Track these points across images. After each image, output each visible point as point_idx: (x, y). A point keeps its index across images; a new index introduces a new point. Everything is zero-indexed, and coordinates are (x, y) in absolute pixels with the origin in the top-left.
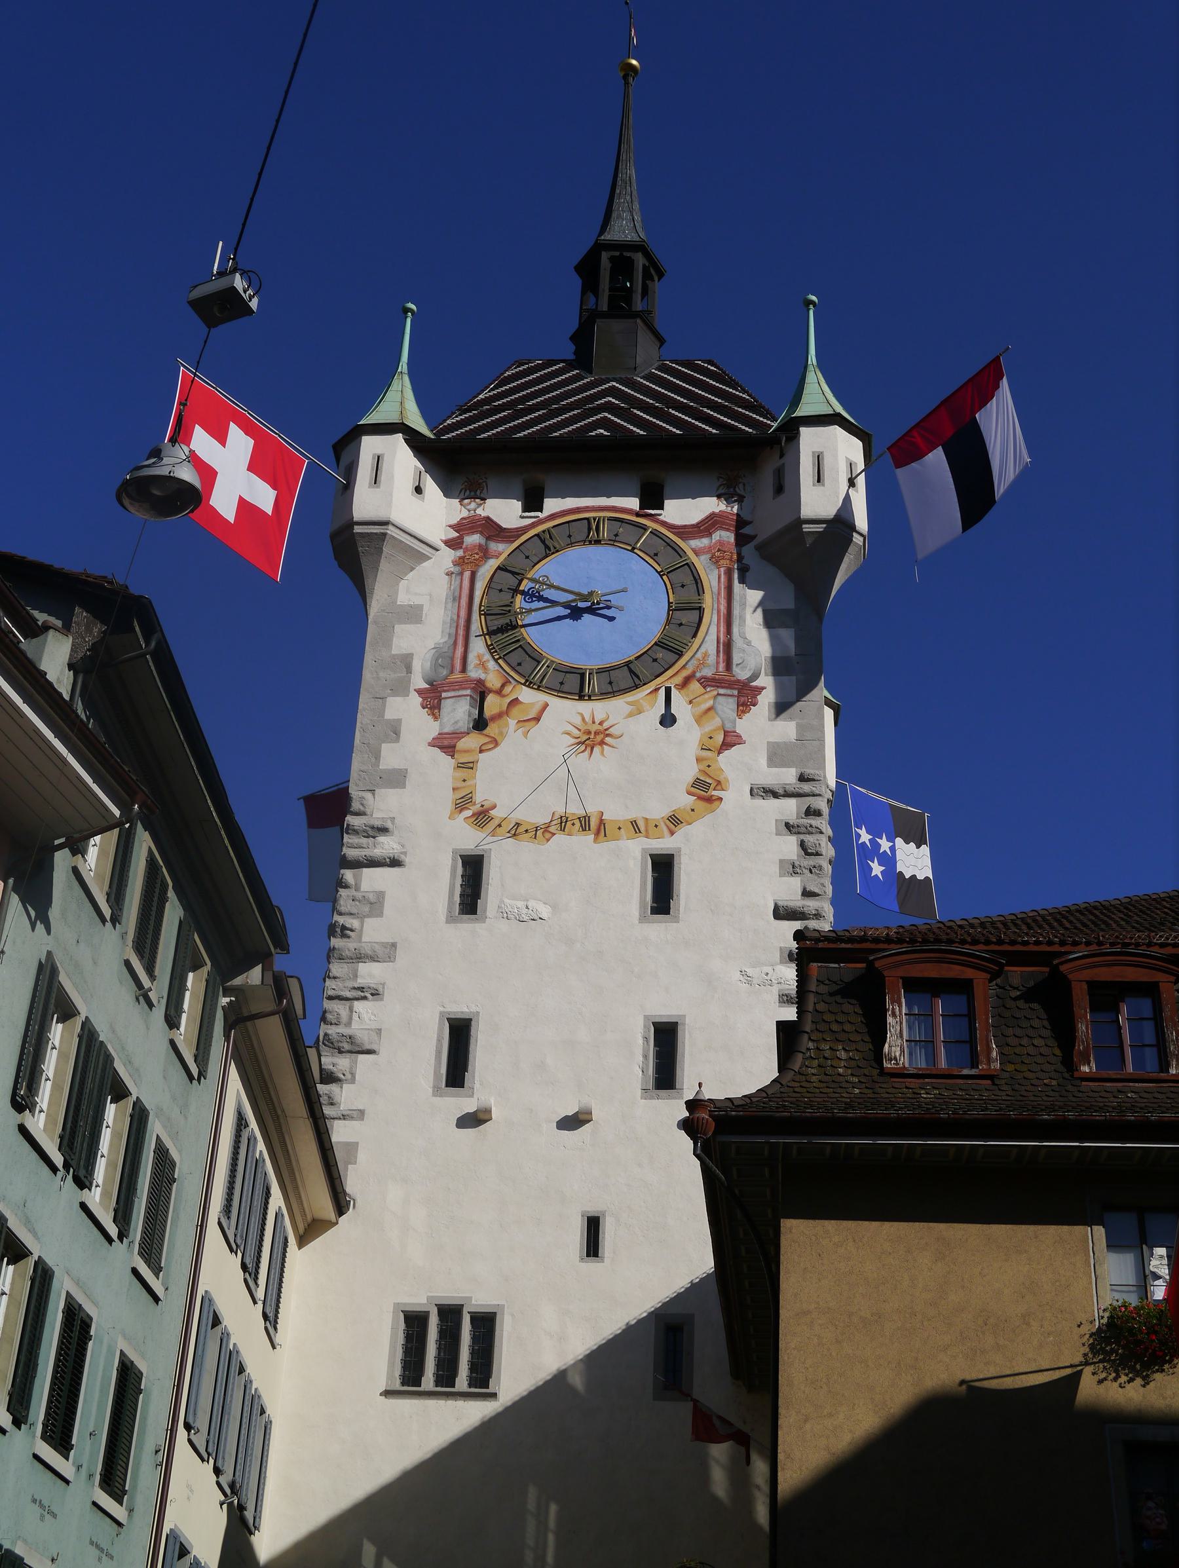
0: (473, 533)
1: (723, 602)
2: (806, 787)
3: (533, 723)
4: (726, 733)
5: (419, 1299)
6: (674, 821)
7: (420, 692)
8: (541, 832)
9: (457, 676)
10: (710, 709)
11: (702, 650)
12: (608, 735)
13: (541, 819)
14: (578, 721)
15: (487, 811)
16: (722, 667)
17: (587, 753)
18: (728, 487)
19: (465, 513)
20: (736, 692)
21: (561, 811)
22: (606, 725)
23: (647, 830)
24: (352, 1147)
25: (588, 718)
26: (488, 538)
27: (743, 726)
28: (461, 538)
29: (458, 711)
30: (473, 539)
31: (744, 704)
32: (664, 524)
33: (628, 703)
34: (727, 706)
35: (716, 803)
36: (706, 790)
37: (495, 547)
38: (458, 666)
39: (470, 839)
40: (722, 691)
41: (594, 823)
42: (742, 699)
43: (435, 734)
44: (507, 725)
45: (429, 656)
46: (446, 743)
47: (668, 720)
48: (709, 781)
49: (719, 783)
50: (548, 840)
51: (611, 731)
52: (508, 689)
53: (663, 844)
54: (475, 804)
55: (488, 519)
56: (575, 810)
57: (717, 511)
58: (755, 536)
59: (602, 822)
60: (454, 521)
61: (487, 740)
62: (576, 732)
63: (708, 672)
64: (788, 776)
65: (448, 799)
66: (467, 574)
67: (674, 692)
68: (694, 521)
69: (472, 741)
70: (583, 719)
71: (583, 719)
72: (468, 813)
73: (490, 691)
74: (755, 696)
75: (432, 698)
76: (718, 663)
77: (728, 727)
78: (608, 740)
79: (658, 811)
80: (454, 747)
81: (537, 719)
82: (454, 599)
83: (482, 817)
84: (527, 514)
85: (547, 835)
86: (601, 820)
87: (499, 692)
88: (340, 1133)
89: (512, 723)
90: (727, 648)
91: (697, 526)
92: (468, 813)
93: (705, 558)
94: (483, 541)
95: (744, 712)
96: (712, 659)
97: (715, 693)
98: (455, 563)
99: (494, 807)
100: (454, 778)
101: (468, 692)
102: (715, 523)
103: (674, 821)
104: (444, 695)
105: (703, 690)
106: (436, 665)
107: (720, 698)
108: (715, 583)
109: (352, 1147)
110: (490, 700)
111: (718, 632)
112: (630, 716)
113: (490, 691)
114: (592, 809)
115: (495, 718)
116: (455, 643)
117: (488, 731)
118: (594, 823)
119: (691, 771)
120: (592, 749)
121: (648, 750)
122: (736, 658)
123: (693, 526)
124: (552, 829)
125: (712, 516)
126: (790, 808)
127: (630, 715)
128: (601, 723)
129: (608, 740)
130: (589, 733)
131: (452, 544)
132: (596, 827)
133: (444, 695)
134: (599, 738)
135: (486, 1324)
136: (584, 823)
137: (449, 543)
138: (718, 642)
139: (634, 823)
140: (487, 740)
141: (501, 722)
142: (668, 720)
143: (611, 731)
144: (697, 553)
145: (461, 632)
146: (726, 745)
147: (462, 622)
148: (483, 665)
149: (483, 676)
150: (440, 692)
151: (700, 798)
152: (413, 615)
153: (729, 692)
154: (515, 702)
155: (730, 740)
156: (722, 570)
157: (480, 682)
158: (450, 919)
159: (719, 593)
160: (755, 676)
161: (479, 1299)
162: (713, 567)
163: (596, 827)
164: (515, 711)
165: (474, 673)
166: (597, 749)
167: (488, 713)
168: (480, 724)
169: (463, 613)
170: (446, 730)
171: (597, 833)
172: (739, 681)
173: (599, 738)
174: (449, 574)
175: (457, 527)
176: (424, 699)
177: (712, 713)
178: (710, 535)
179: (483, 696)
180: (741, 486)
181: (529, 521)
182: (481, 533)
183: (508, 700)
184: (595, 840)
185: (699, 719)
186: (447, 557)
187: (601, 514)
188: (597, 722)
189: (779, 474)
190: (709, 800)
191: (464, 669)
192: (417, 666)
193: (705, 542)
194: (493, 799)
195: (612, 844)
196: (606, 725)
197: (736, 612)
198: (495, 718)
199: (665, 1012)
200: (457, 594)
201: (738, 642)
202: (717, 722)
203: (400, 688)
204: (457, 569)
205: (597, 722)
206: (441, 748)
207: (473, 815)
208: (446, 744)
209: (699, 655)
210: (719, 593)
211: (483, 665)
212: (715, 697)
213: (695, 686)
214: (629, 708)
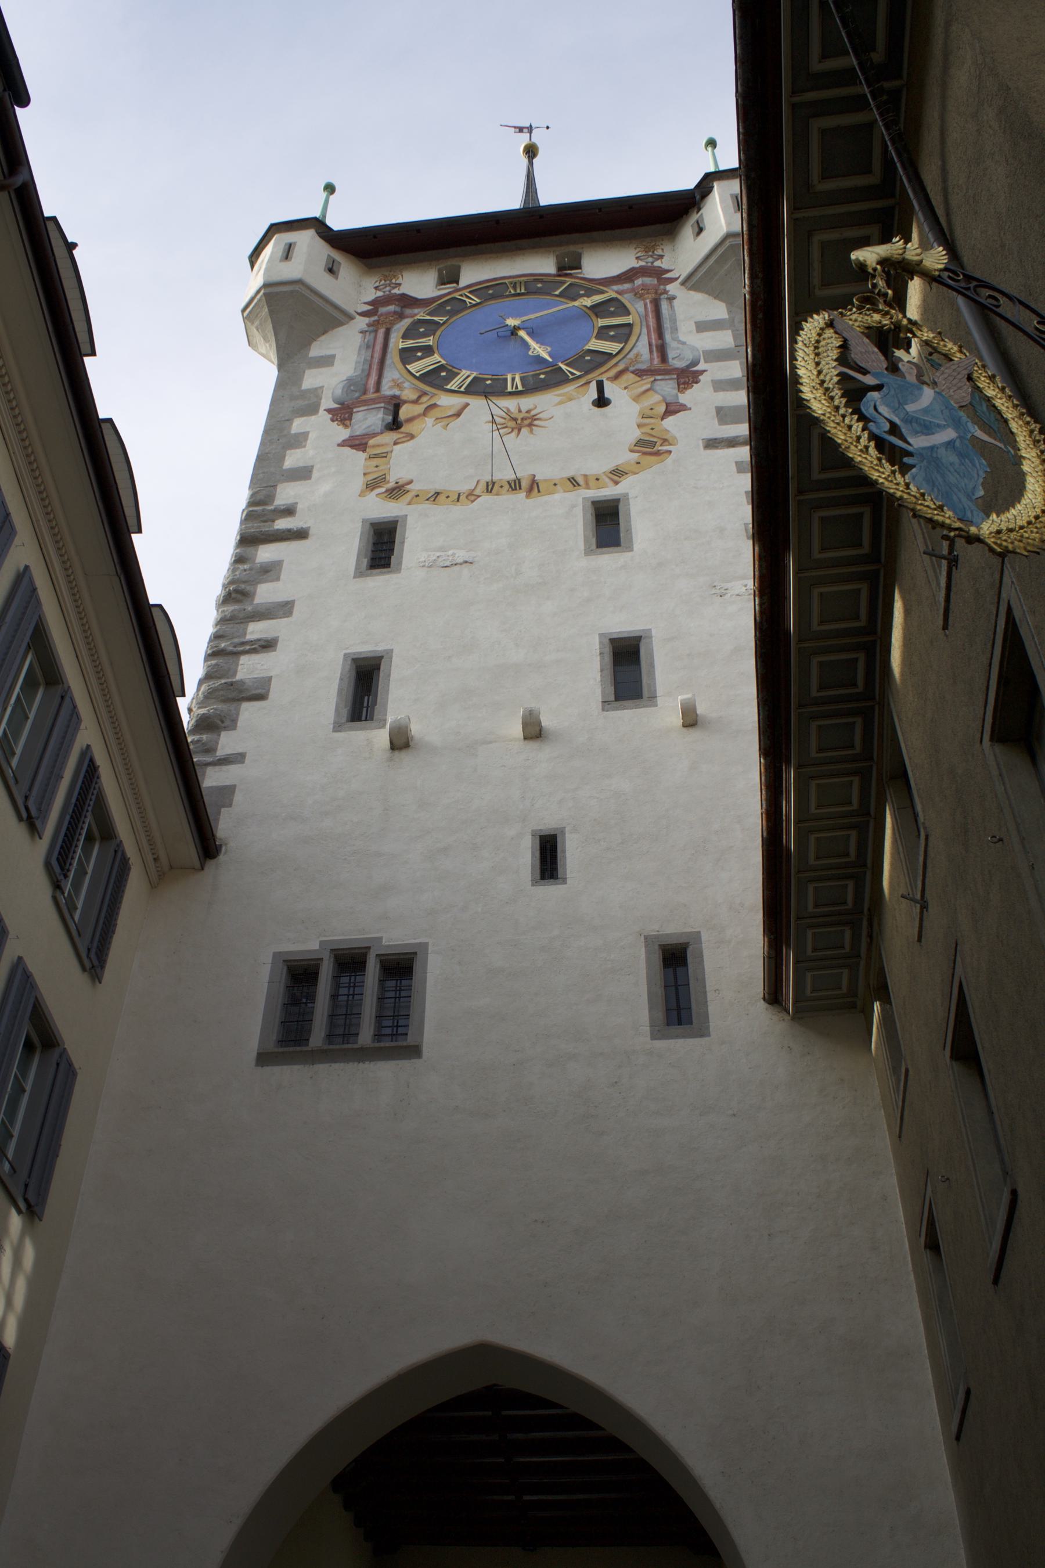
4: (667, 405)
5: (306, 943)
6: (618, 474)
7: (329, 411)
9: (371, 395)
11: (635, 351)
13: (465, 487)
15: (403, 486)
17: (514, 434)
19: (380, 294)
22: (533, 413)
24: (227, 793)
35: (666, 455)
36: (651, 447)
39: (381, 509)
40: (659, 377)
41: (525, 484)
42: (682, 380)
47: (602, 402)
50: (473, 501)
53: (608, 492)
55: (403, 295)
57: (637, 266)
58: (677, 279)
65: (359, 482)
73: (405, 402)
75: (342, 413)
77: (669, 399)
78: (536, 422)
80: (366, 444)
82: (368, 347)
83: (397, 491)
85: (473, 498)
88: (211, 779)
90: (662, 351)
92: (383, 490)
94: (398, 309)
95: (685, 389)
97: (652, 379)
100: (366, 467)
101: (382, 405)
102: (637, 273)
103: (618, 474)
109: (227, 793)
117: (402, 429)
118: (525, 484)
120: (519, 430)
121: (580, 432)
122: (671, 354)
124: (477, 492)
125: (632, 269)
131: (363, 314)
134: (527, 422)
135: (401, 968)
136: (515, 485)
137: (363, 314)
138: (650, 345)
142: (602, 402)
145: (375, 367)
149: (397, 393)
155: (672, 409)
158: (359, 574)
159: (646, 315)
160: (695, 363)
161: (395, 937)
165: (387, 390)
168: (395, 425)
169: (377, 355)
172: (677, 369)
173: (527, 422)
178: (632, 281)
179: (397, 407)
184: (527, 497)
186: (362, 322)
187: (521, 279)
193: (627, 286)
199: (622, 624)
200: (371, 344)
202: (657, 398)
206: (352, 447)
207: (387, 491)
208: (357, 443)
209: (631, 355)
210: (646, 315)
213: (630, 377)
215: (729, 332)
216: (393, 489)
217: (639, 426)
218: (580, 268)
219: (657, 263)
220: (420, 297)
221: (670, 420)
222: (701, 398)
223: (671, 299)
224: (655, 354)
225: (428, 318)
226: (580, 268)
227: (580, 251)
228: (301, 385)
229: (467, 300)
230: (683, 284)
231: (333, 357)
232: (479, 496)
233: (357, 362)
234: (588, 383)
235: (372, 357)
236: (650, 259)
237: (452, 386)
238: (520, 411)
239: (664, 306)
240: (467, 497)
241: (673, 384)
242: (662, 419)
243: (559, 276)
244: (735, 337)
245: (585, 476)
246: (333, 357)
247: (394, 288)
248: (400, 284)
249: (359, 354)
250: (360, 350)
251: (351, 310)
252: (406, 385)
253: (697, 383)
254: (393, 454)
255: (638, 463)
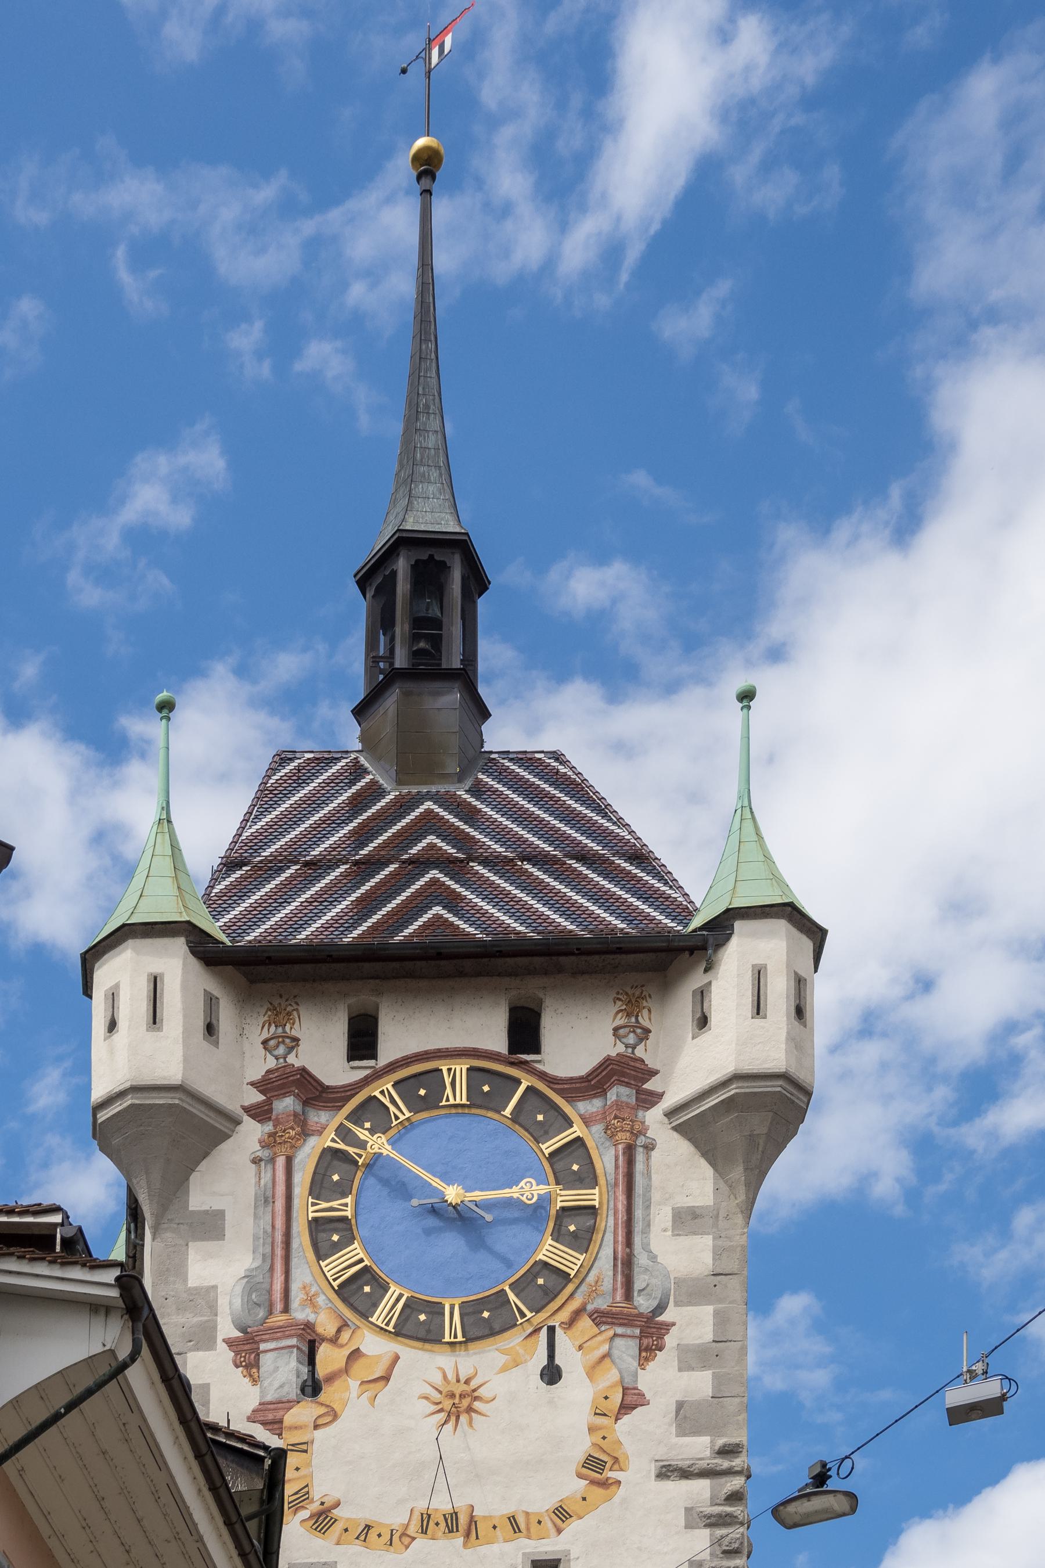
0: (284, 1095)
1: (622, 1198)
2: (725, 1464)
3: (383, 1383)
4: (625, 1390)
6: (562, 1514)
7: (230, 1343)
8: (399, 1538)
9: (279, 1319)
10: (604, 1357)
12: (476, 1398)
13: (397, 1519)
14: (437, 1379)
16: (619, 1296)
17: (449, 1426)
18: (629, 1015)
19: (271, 1063)
20: (637, 1331)
21: (422, 1505)
22: (474, 1384)
23: (528, 1529)
25: (451, 1376)
26: (306, 1103)
27: (647, 1380)
28: (269, 1102)
29: (282, 1369)
30: (286, 1104)
31: (648, 1349)
32: (543, 1076)
33: (504, 1352)
34: (626, 1349)
35: (614, 1488)
37: (318, 1117)
38: (279, 1306)
40: (620, 1330)
41: (463, 1520)
43: (254, 1404)
44: (348, 1388)
45: (239, 1289)
46: (270, 1417)
47: (552, 1374)
48: (604, 1458)
49: (616, 1460)
50: (407, 1547)
51: (481, 1392)
52: (345, 1336)
54: (312, 1501)
55: (303, 1070)
56: (441, 1504)
57: (614, 1054)
58: (660, 1096)
59: (472, 1521)
60: (257, 1073)
61: (322, 1410)
62: (436, 1396)
63: (601, 1304)
64: (698, 1448)
66: (281, 1161)
67: (559, 1332)
68: (583, 1072)
69: (304, 1412)
70: (445, 1377)
71: (445, 1377)
72: (305, 1514)
73: (323, 1340)
74: (661, 1337)
75: (247, 1351)
76: (615, 1290)
77: (628, 1382)
78: (477, 1405)
79: (539, 1500)
80: (281, 1422)
81: (386, 1378)
84: (357, 1063)
85: (406, 1540)
86: (472, 1517)
87: (334, 1341)
89: (354, 1384)
90: (626, 1265)
91: (586, 1079)
92: (305, 1514)
93: (598, 1128)
94: (299, 1108)
95: (647, 1359)
96: (607, 1284)
97: (611, 1333)
98: (264, 1145)
99: (337, 1504)
101: (294, 1341)
102: (613, 1073)
103: (562, 1514)
104: (263, 1346)
105: (596, 1330)
106: (251, 1305)
107: (618, 1341)
108: (610, 1167)
110: (324, 1352)
111: (615, 1242)
112: (501, 1369)
113: (323, 1340)
114: (460, 1504)
115: (331, 1378)
116: (272, 1269)
117: (322, 1397)
118: (463, 1520)
119: (582, 1446)
120: (458, 1418)
123: (581, 1078)
124: (412, 1531)
125: (608, 1061)
126: (700, 1491)
127: (504, 1369)
128: (467, 1382)
129: (477, 1405)
130: (452, 1395)
132: (463, 1526)
133: (263, 1346)
134: (465, 1403)
136: (451, 1522)
138: (615, 1259)
139: (512, 1520)
140: (322, 1410)
141: (337, 1384)
142: (552, 1374)
143: (481, 1392)
144: (587, 1121)
145: (279, 1252)
146: (626, 1408)
147: (279, 1237)
148: (310, 1301)
149: (312, 1318)
150: (257, 1343)
151: (593, 1482)
152: (211, 1226)
153: (629, 1331)
154: (355, 1354)
155: (631, 1401)
156: (620, 1147)
157: (309, 1326)
159: (616, 1184)
160: (661, 1308)
162: (608, 1143)
163: (463, 1526)
164: (358, 1367)
165: (300, 1314)
166: (464, 1418)
167: (321, 1372)
168: (312, 1388)
170: (269, 1398)
171: (467, 1535)
173: (465, 1403)
174: (256, 1161)
175: (262, 1085)
176: (237, 1353)
177: (607, 1360)
178: (604, 1093)
180: (645, 1012)
181: (361, 1074)
182: (297, 1096)
183: (346, 1352)
185: (592, 1371)
186: (251, 1134)
188: (463, 1379)
189: (702, 994)
190: (604, 1484)
191: (286, 1309)
192: (223, 1304)
194: (336, 1494)
195: (483, 1550)
196: (474, 1384)
197: (638, 1213)
198: (331, 1378)
200: (269, 1193)
201: (641, 1259)
203: (204, 1338)
204: (265, 1154)
205: (463, 1379)
207: (311, 1517)
210: (616, 1184)
211: (310, 1301)
212: (612, 1339)
213: (585, 1323)
214: (501, 1359)
215: (708, 1241)
216: (320, 1514)
217: (591, 1430)
218: (537, 1051)
219: (639, 1052)
220: (328, 1082)
221: (626, 1419)
222: (666, 1380)
223: (649, 1148)
224: (619, 1277)
225: (341, 1146)
226: (537, 1051)
227: (541, 995)
228: (185, 1280)
229: (392, 1108)
230: (670, 1114)
231: (220, 1214)
232: (414, 1539)
233: (256, 1238)
234: (537, 1330)
235: (273, 1227)
236: (631, 1039)
237: (378, 1317)
238: (458, 1381)
239: (640, 1156)
240: (400, 1537)
241: (633, 1345)
242: (617, 1420)
243: (512, 1064)
244: (718, 1253)
245: (527, 1514)
246: (220, 1214)
247: (291, 1049)
248: (296, 1040)
249: (256, 1216)
250: (256, 1207)
251: (234, 1106)
252: (321, 1300)
253: (660, 1350)
254: (316, 1446)
255: (584, 1499)
